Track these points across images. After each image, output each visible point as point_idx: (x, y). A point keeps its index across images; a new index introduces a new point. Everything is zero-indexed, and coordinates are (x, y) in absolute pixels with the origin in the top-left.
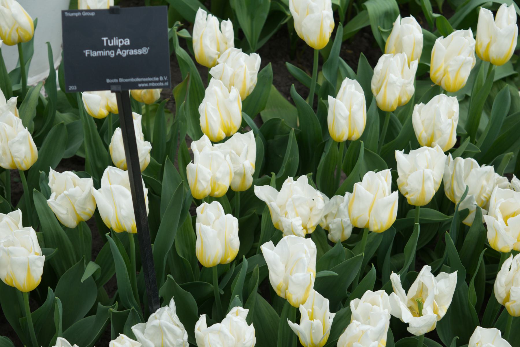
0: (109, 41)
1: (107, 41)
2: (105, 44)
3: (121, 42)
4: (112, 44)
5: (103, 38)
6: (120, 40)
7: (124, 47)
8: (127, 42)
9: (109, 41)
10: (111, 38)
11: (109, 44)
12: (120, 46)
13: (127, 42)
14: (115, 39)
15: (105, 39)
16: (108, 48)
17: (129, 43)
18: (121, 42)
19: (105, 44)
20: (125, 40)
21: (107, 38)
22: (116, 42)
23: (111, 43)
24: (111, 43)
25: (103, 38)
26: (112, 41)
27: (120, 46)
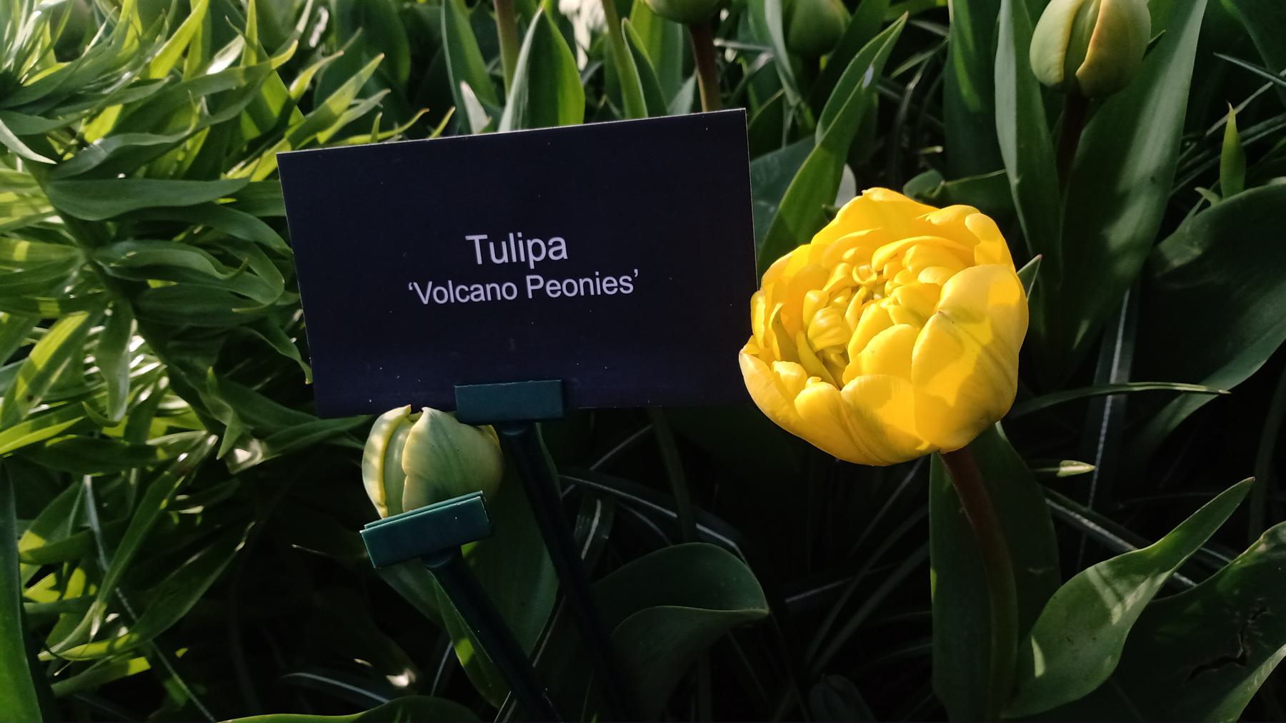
0: (492, 245)
2: (480, 261)
4: (505, 258)
5: (469, 238)
6: (530, 243)
7: (548, 269)
8: (559, 249)
9: (492, 245)
10: (498, 237)
12: (532, 266)
13: (559, 249)
14: (511, 235)
15: (476, 238)
17: (564, 255)
19: (480, 261)
20: (550, 243)
21: (485, 237)
23: (499, 255)
24: (499, 255)
25: (469, 238)
26: (504, 244)
27: (532, 266)
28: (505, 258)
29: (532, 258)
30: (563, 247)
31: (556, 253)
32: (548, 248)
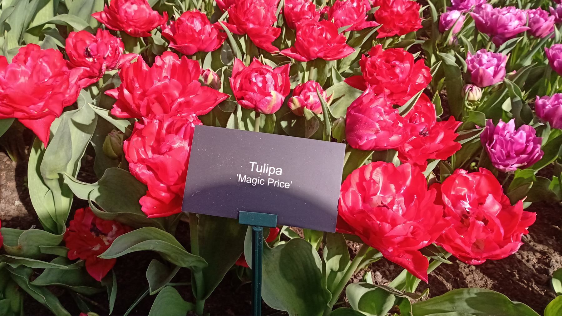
1: (255, 165)
2: (252, 170)
3: (272, 171)
4: (261, 171)
6: (270, 168)
7: (274, 177)
10: (260, 164)
11: (257, 171)
13: (279, 172)
15: (253, 163)
16: (254, 175)
17: (281, 174)
18: (272, 171)
19: (252, 170)
22: (265, 169)
23: (259, 170)
24: (259, 170)
28: (261, 171)
29: (270, 173)
30: (281, 171)
31: (278, 173)
32: (276, 171)
